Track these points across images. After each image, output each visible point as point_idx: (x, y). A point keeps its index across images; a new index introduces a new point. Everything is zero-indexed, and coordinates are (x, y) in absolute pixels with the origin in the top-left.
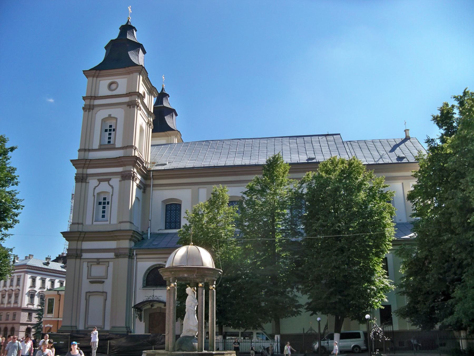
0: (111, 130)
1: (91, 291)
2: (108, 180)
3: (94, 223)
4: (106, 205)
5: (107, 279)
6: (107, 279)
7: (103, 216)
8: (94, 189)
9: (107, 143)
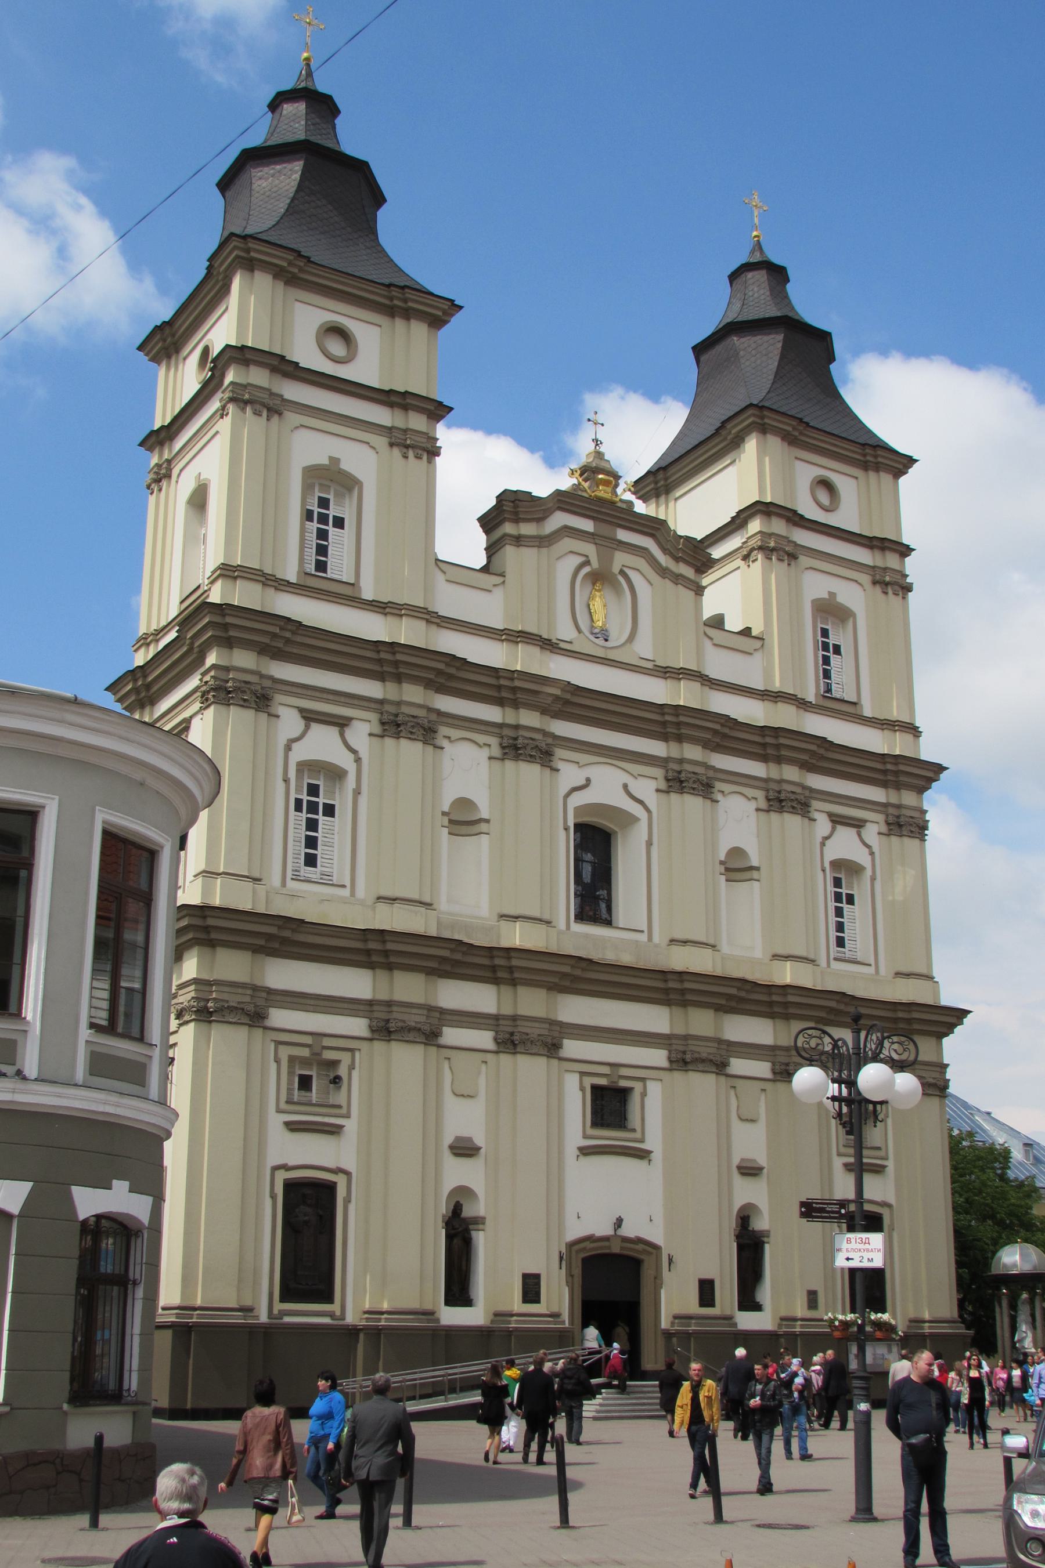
0: (322, 520)
1: (291, 1163)
2: (341, 724)
3: (291, 884)
4: (321, 818)
5: (348, 1116)
6: (348, 1116)
7: (311, 861)
8: (288, 748)
9: (311, 568)
